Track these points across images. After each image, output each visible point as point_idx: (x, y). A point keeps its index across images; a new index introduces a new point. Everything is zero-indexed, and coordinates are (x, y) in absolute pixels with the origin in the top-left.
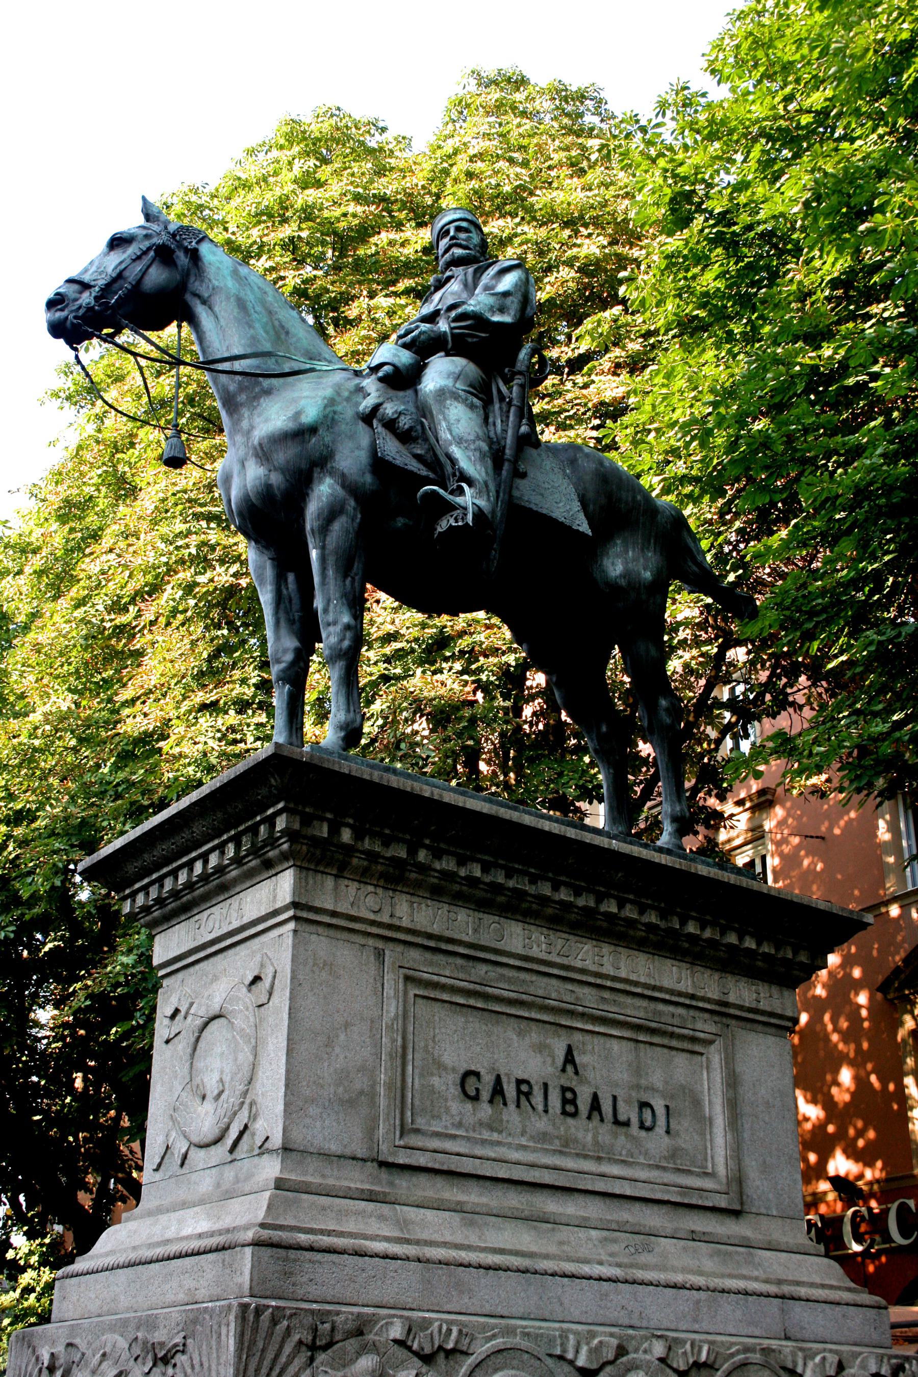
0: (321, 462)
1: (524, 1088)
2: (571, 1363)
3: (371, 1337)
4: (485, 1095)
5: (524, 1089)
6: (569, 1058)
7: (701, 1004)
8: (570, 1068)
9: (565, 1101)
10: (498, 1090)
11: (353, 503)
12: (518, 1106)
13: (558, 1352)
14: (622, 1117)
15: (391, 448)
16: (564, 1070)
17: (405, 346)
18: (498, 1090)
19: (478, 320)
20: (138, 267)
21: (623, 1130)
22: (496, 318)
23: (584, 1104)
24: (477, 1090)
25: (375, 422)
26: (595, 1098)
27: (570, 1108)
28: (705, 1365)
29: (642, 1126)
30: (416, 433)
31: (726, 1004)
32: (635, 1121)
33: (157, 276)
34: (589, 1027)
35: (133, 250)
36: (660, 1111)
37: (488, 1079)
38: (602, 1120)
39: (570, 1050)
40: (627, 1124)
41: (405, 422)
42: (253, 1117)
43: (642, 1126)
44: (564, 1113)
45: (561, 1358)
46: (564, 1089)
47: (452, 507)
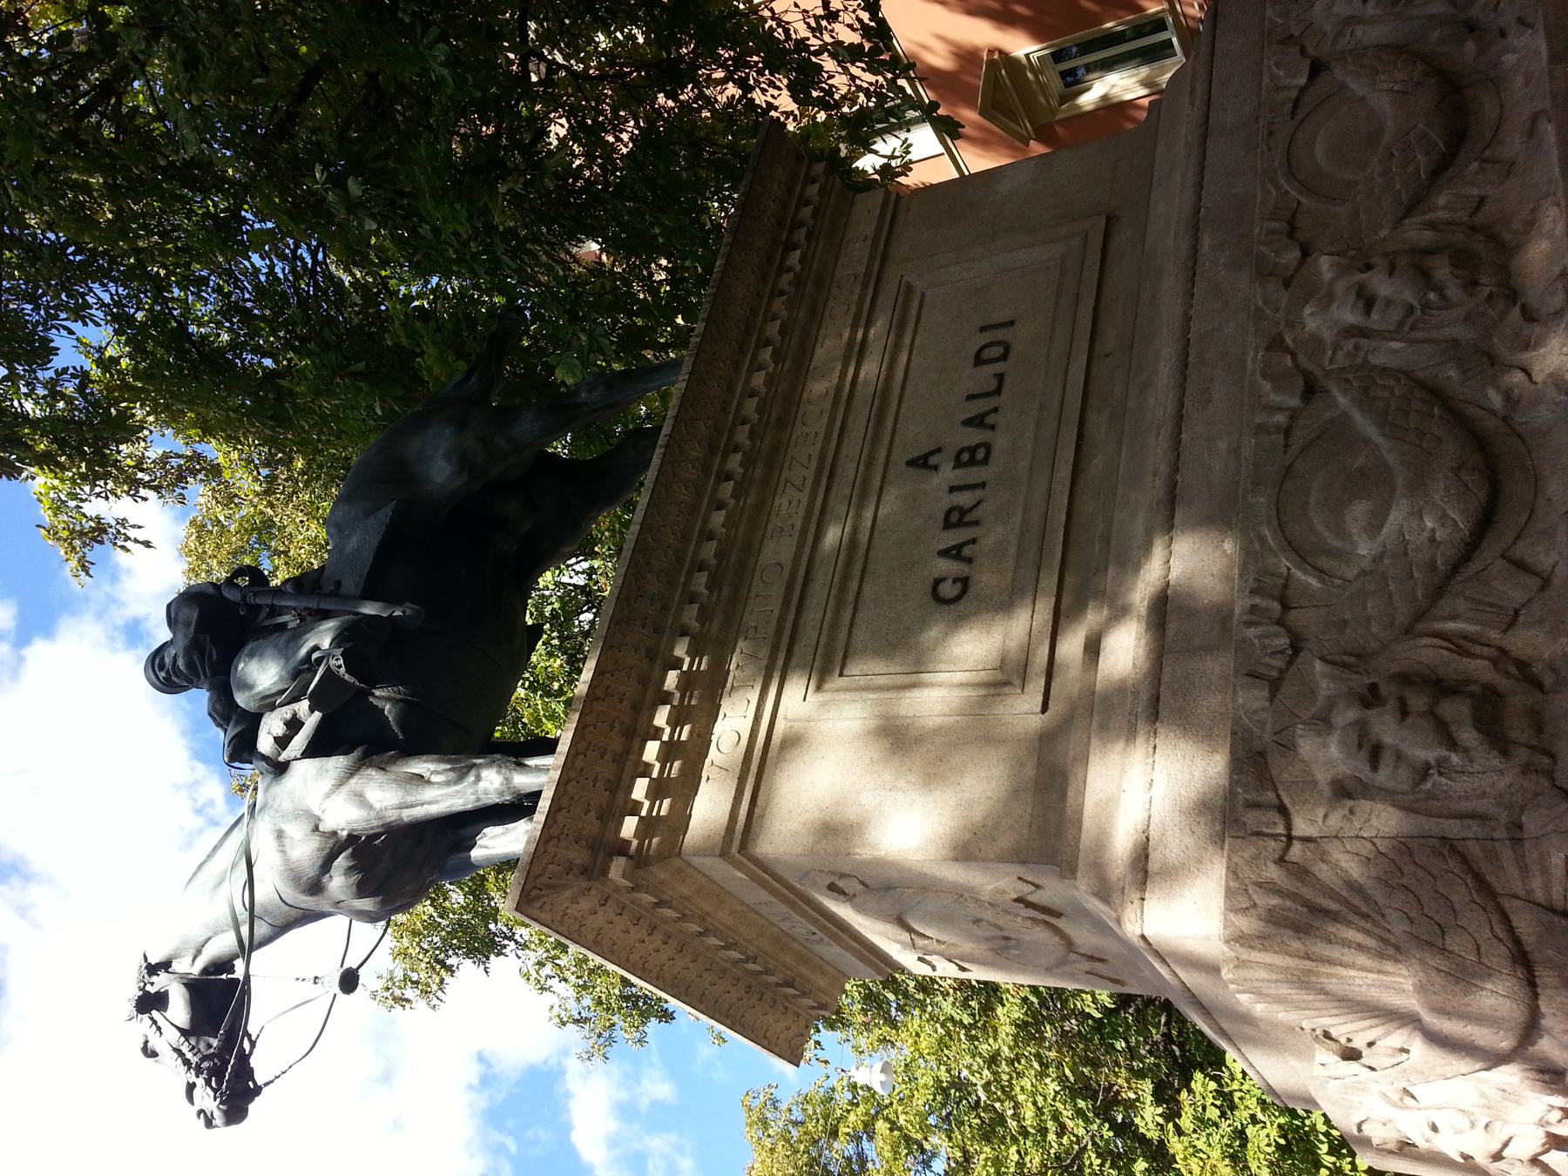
1: (954, 517)
2: (1294, 415)
3: (1267, 737)
5: (956, 518)
7: (867, 305)
8: (933, 460)
9: (972, 462)
12: (977, 523)
13: (1279, 438)
14: (993, 384)
16: (936, 468)
21: (1007, 379)
23: (974, 437)
24: (955, 581)
25: (284, 756)
26: (968, 423)
27: (980, 455)
28: (1291, 222)
29: (1004, 357)
31: (867, 275)
32: (998, 367)
34: (886, 440)
36: (987, 337)
38: (996, 410)
39: (912, 463)
40: (1000, 377)
43: (1004, 357)
45: (1287, 432)
46: (958, 464)
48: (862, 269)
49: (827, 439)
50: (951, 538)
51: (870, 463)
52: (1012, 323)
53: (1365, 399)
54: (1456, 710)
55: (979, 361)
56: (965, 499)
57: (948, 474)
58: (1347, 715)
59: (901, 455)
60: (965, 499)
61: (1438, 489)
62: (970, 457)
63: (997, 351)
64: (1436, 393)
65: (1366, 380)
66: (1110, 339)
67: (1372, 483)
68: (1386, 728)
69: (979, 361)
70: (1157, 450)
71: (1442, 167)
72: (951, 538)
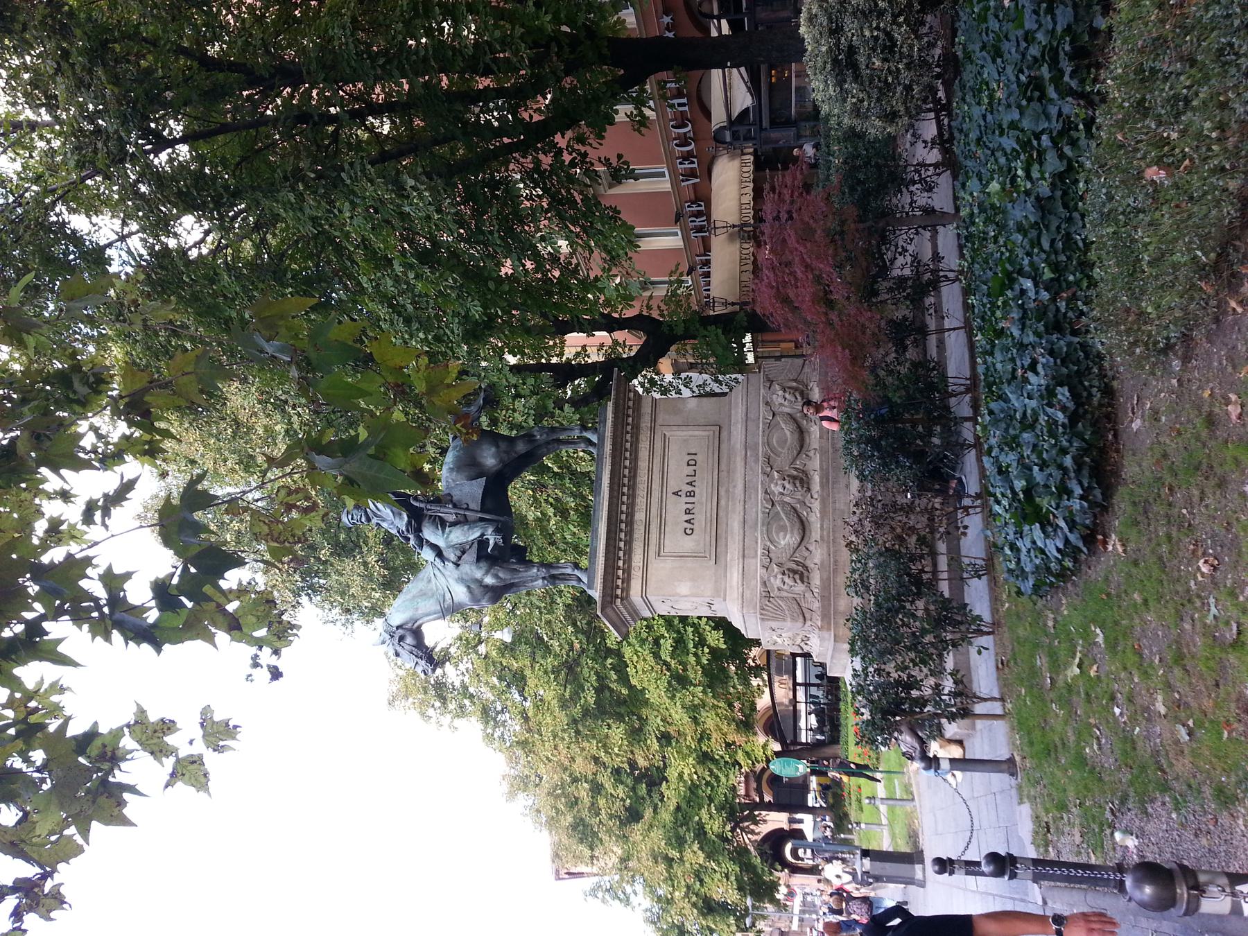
0: (479, 582)
5: (688, 512)
6: (676, 493)
17: (421, 547)
19: (409, 523)
20: (407, 647)
22: (406, 518)
23: (690, 488)
33: (409, 640)
35: (399, 649)
41: (459, 553)
47: (496, 544)
50: (688, 517)
53: (783, 509)
54: (797, 577)
56: (690, 506)
58: (780, 576)
59: (670, 491)
60: (690, 506)
61: (796, 532)
62: (690, 494)
64: (794, 509)
65: (784, 504)
66: (723, 467)
67: (783, 528)
68: (786, 579)
70: (739, 507)
72: (688, 517)
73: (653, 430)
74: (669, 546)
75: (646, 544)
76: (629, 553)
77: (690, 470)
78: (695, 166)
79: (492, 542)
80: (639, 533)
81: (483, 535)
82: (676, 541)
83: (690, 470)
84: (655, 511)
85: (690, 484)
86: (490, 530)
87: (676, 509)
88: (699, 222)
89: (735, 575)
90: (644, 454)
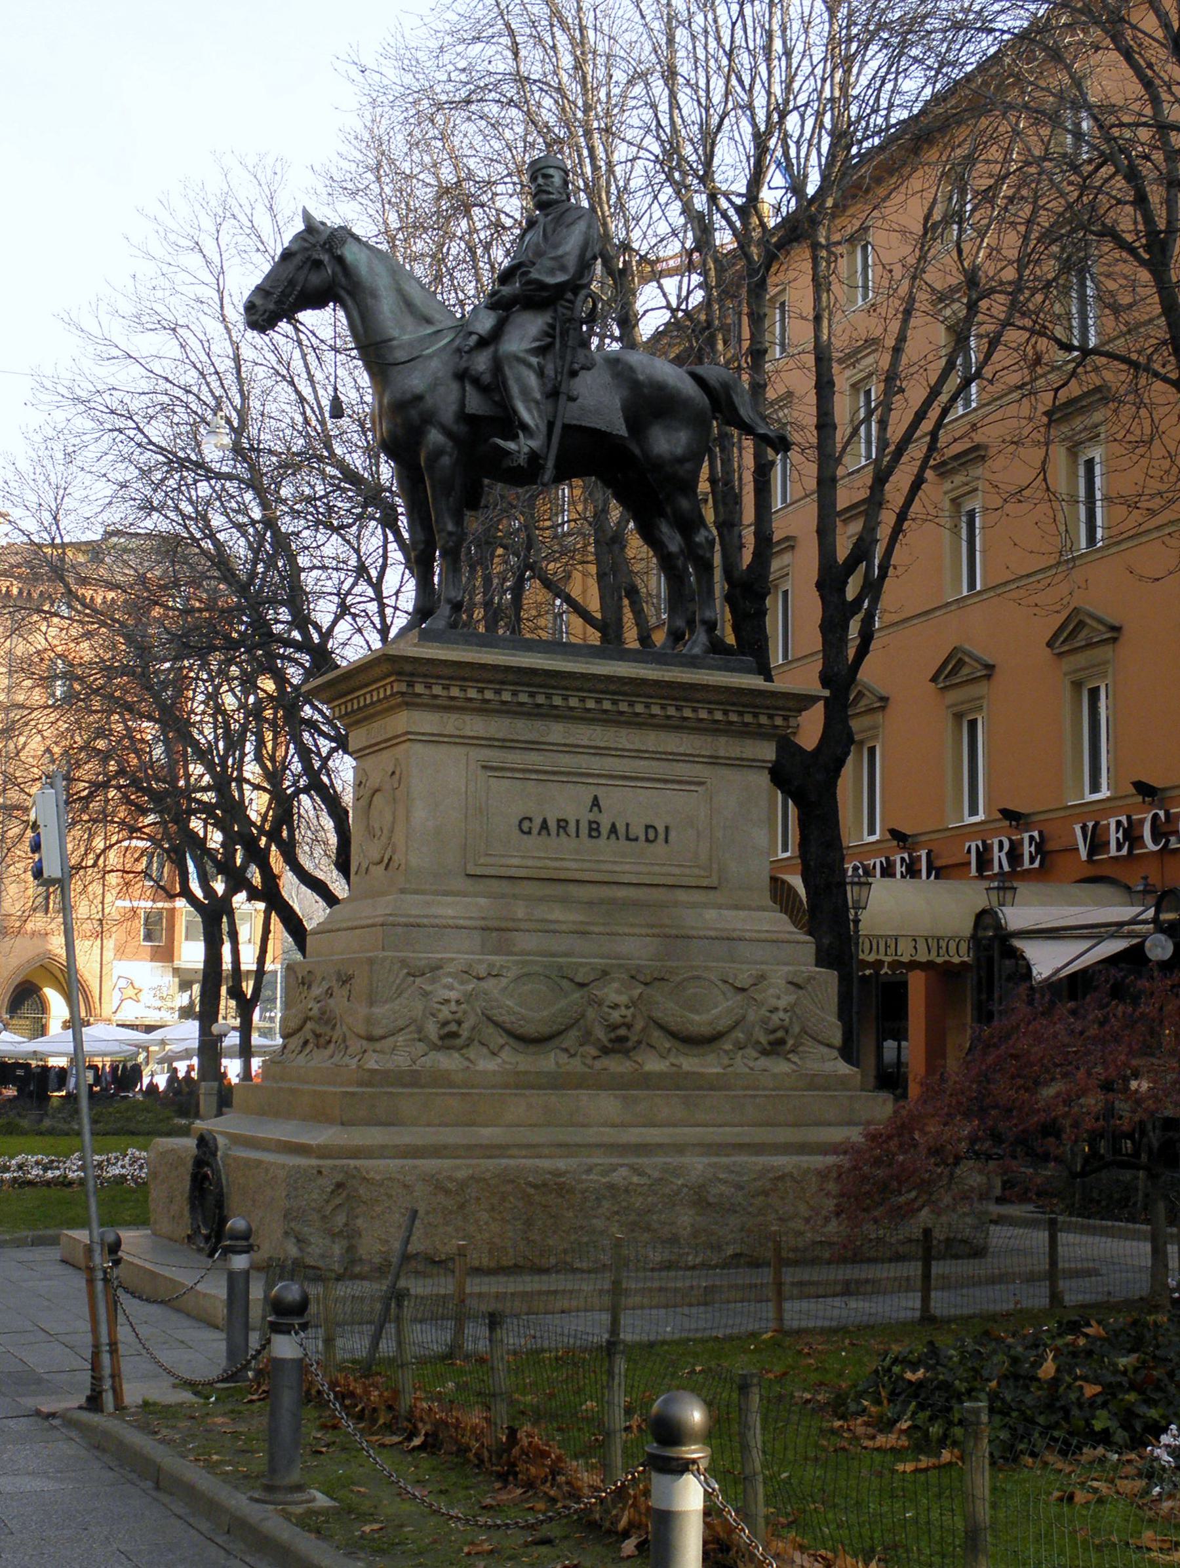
4: (535, 831)
5: (562, 824)
6: (596, 802)
9: (591, 829)
10: (544, 825)
11: (450, 444)
15: (475, 403)
18: (544, 825)
23: (605, 830)
27: (594, 834)
30: (494, 387)
32: (642, 837)
36: (661, 830)
37: (538, 822)
39: (596, 798)
40: (636, 839)
41: (487, 379)
42: (394, 852)
43: (647, 840)
44: (590, 836)
46: (590, 823)
47: (507, 453)
48: (722, 753)
49: (616, 749)
51: (599, 776)
52: (667, 841)
55: (647, 827)
57: (586, 817)
59: (600, 792)
60: (572, 828)
62: (594, 829)
63: (651, 836)
69: (647, 827)
71: (673, 1035)
72: (552, 825)
73: (714, 761)
74: (500, 786)
75: (505, 744)
76: (484, 709)
77: (638, 830)
78: (1113, 852)
79: (511, 446)
80: (523, 729)
81: (524, 427)
82: (511, 800)
83: (638, 830)
84: (566, 761)
85: (613, 829)
86: (534, 444)
87: (569, 803)
88: (999, 858)
89: (450, 912)
90: (673, 742)
